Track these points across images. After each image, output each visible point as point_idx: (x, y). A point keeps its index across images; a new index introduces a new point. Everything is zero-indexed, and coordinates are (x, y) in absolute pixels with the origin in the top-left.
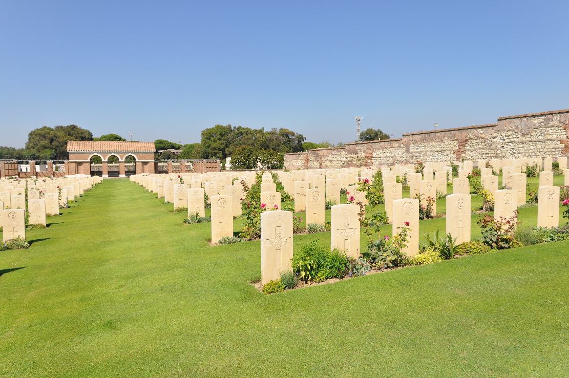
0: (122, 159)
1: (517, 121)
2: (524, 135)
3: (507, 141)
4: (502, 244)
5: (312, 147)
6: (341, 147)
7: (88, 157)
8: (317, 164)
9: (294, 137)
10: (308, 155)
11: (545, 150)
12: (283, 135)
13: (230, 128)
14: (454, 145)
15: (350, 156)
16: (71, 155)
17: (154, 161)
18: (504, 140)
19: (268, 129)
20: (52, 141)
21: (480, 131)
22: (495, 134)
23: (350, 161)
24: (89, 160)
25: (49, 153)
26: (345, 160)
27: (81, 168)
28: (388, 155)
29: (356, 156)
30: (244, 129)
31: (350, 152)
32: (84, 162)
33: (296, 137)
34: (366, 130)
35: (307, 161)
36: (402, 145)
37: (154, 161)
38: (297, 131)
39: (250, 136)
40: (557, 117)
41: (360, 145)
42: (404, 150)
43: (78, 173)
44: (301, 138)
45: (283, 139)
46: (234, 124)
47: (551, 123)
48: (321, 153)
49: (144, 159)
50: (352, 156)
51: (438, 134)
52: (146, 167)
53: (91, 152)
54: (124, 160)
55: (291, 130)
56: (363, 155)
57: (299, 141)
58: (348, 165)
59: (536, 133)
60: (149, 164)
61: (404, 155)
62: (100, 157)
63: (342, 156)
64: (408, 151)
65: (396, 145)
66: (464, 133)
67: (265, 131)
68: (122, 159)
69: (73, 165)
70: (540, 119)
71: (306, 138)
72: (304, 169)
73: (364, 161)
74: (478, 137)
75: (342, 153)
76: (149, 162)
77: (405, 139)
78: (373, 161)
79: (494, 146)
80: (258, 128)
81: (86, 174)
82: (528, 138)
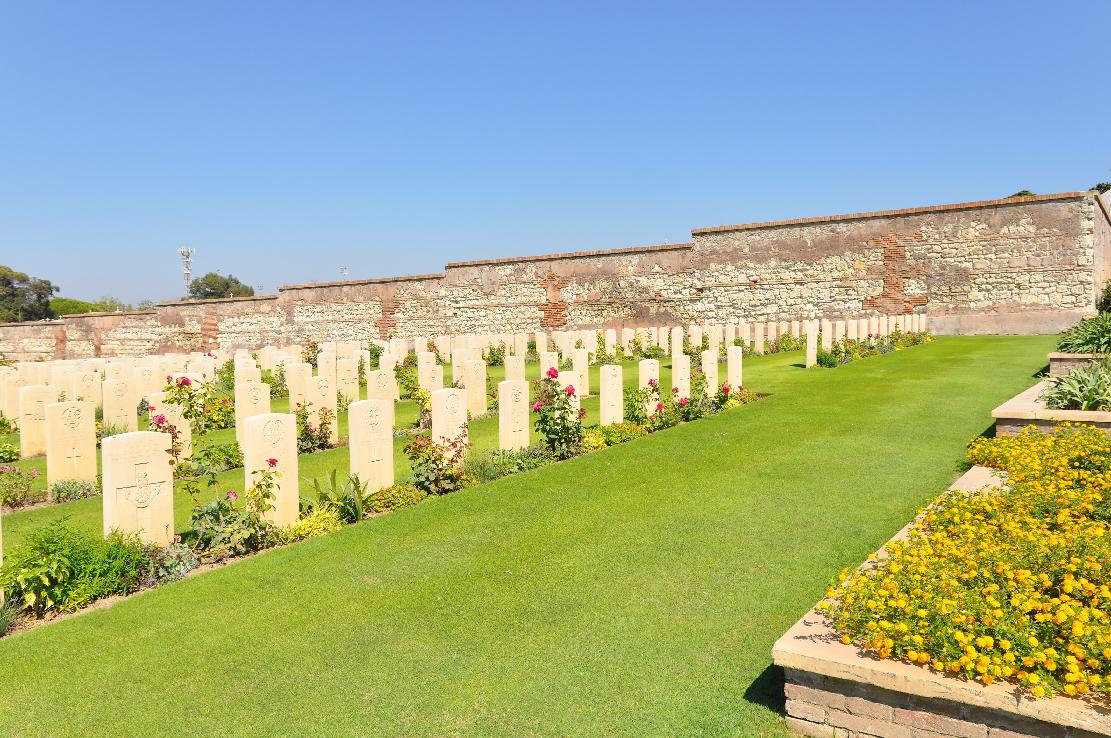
1: (474, 270)
2: (487, 295)
3: (461, 304)
4: (439, 484)
5: (75, 309)
6: (145, 312)
8: (86, 347)
10: (65, 328)
11: (518, 321)
14: (376, 312)
15: (168, 330)
18: (457, 302)
21: (418, 285)
22: (443, 292)
23: (167, 339)
26: (155, 337)
28: (250, 328)
31: (166, 321)
33: (36, 287)
35: (62, 340)
36: (278, 308)
38: (36, 272)
40: (532, 268)
42: (283, 319)
44: (44, 289)
47: (524, 277)
48: (97, 322)
50: (173, 329)
51: (345, 289)
55: (17, 269)
56: (196, 328)
57: (40, 297)
58: (165, 347)
59: (503, 292)
61: (282, 329)
63: (151, 331)
64: (290, 321)
65: (265, 307)
66: (392, 289)
70: (509, 269)
71: (58, 290)
72: (54, 358)
73: (201, 340)
74: (417, 298)
77: (284, 297)
78: (219, 340)
79: (441, 314)
82: (493, 300)
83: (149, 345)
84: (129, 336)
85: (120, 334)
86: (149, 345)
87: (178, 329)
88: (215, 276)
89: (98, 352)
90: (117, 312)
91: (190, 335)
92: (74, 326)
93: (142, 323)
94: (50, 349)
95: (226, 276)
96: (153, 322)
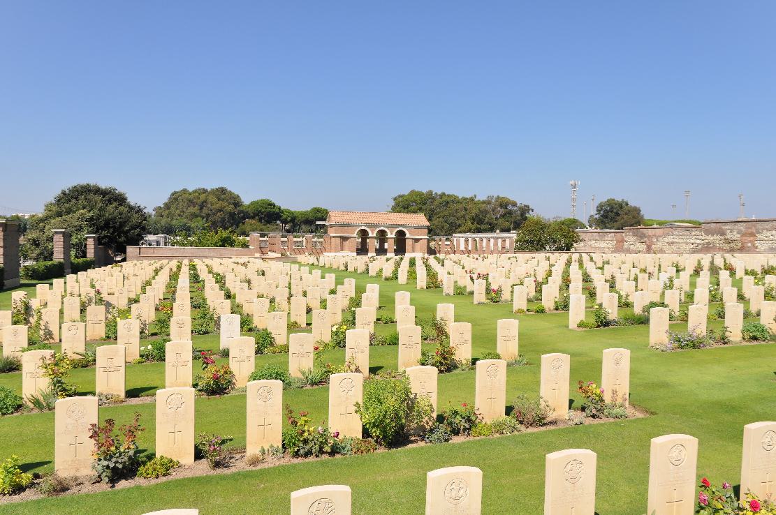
6: (698, 225)
8: (644, 247)
9: (516, 208)
10: (624, 234)
12: (501, 206)
13: (431, 195)
15: (710, 238)
19: (481, 197)
20: (201, 208)
23: (709, 243)
25: (199, 223)
26: (698, 242)
29: (723, 237)
30: (448, 196)
31: (708, 232)
33: (520, 208)
34: (606, 200)
35: (623, 241)
37: (427, 237)
39: (454, 206)
41: (733, 224)
45: (502, 211)
46: (438, 190)
48: (650, 232)
49: (416, 235)
50: (715, 237)
52: (418, 245)
54: (375, 235)
55: (512, 198)
56: (737, 236)
58: (707, 248)
60: (421, 241)
63: (698, 238)
67: (476, 199)
69: (338, 240)
71: (533, 210)
73: (740, 245)
75: (693, 233)
76: (421, 239)
80: (468, 196)
83: (692, 246)
84: (676, 240)
85: (669, 239)
86: (692, 246)
87: (719, 237)
88: (614, 200)
89: (649, 250)
90: (655, 226)
91: (728, 242)
92: (631, 234)
93: (688, 233)
94: (611, 246)
95: (620, 200)
96: (698, 233)
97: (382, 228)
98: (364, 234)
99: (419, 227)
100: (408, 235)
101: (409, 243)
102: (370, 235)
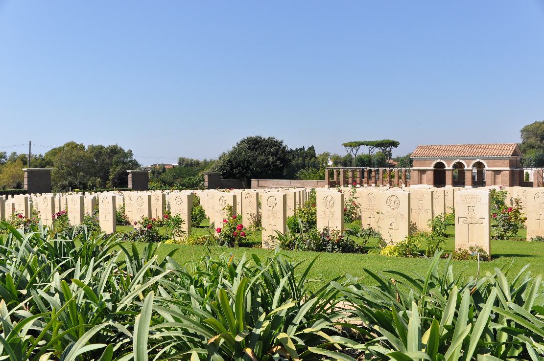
0: (468, 166)
7: (431, 163)
16: (414, 162)
17: (508, 168)
24: (432, 168)
27: (424, 176)
32: (426, 171)
43: (420, 183)
49: (496, 166)
53: (435, 159)
62: (444, 164)
68: (468, 166)
76: (502, 171)
81: (428, 184)
97: (478, 160)
98: (439, 167)
99: (500, 158)
100: (487, 168)
101: (488, 177)
102: (447, 168)
